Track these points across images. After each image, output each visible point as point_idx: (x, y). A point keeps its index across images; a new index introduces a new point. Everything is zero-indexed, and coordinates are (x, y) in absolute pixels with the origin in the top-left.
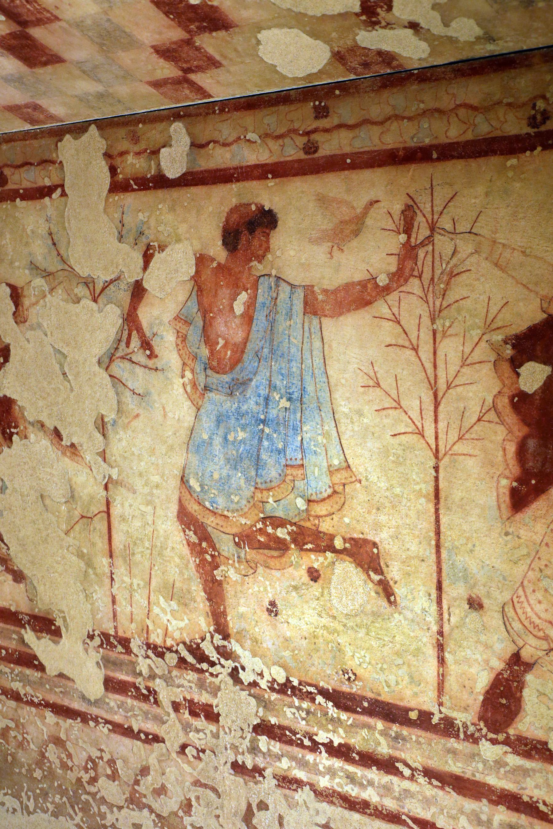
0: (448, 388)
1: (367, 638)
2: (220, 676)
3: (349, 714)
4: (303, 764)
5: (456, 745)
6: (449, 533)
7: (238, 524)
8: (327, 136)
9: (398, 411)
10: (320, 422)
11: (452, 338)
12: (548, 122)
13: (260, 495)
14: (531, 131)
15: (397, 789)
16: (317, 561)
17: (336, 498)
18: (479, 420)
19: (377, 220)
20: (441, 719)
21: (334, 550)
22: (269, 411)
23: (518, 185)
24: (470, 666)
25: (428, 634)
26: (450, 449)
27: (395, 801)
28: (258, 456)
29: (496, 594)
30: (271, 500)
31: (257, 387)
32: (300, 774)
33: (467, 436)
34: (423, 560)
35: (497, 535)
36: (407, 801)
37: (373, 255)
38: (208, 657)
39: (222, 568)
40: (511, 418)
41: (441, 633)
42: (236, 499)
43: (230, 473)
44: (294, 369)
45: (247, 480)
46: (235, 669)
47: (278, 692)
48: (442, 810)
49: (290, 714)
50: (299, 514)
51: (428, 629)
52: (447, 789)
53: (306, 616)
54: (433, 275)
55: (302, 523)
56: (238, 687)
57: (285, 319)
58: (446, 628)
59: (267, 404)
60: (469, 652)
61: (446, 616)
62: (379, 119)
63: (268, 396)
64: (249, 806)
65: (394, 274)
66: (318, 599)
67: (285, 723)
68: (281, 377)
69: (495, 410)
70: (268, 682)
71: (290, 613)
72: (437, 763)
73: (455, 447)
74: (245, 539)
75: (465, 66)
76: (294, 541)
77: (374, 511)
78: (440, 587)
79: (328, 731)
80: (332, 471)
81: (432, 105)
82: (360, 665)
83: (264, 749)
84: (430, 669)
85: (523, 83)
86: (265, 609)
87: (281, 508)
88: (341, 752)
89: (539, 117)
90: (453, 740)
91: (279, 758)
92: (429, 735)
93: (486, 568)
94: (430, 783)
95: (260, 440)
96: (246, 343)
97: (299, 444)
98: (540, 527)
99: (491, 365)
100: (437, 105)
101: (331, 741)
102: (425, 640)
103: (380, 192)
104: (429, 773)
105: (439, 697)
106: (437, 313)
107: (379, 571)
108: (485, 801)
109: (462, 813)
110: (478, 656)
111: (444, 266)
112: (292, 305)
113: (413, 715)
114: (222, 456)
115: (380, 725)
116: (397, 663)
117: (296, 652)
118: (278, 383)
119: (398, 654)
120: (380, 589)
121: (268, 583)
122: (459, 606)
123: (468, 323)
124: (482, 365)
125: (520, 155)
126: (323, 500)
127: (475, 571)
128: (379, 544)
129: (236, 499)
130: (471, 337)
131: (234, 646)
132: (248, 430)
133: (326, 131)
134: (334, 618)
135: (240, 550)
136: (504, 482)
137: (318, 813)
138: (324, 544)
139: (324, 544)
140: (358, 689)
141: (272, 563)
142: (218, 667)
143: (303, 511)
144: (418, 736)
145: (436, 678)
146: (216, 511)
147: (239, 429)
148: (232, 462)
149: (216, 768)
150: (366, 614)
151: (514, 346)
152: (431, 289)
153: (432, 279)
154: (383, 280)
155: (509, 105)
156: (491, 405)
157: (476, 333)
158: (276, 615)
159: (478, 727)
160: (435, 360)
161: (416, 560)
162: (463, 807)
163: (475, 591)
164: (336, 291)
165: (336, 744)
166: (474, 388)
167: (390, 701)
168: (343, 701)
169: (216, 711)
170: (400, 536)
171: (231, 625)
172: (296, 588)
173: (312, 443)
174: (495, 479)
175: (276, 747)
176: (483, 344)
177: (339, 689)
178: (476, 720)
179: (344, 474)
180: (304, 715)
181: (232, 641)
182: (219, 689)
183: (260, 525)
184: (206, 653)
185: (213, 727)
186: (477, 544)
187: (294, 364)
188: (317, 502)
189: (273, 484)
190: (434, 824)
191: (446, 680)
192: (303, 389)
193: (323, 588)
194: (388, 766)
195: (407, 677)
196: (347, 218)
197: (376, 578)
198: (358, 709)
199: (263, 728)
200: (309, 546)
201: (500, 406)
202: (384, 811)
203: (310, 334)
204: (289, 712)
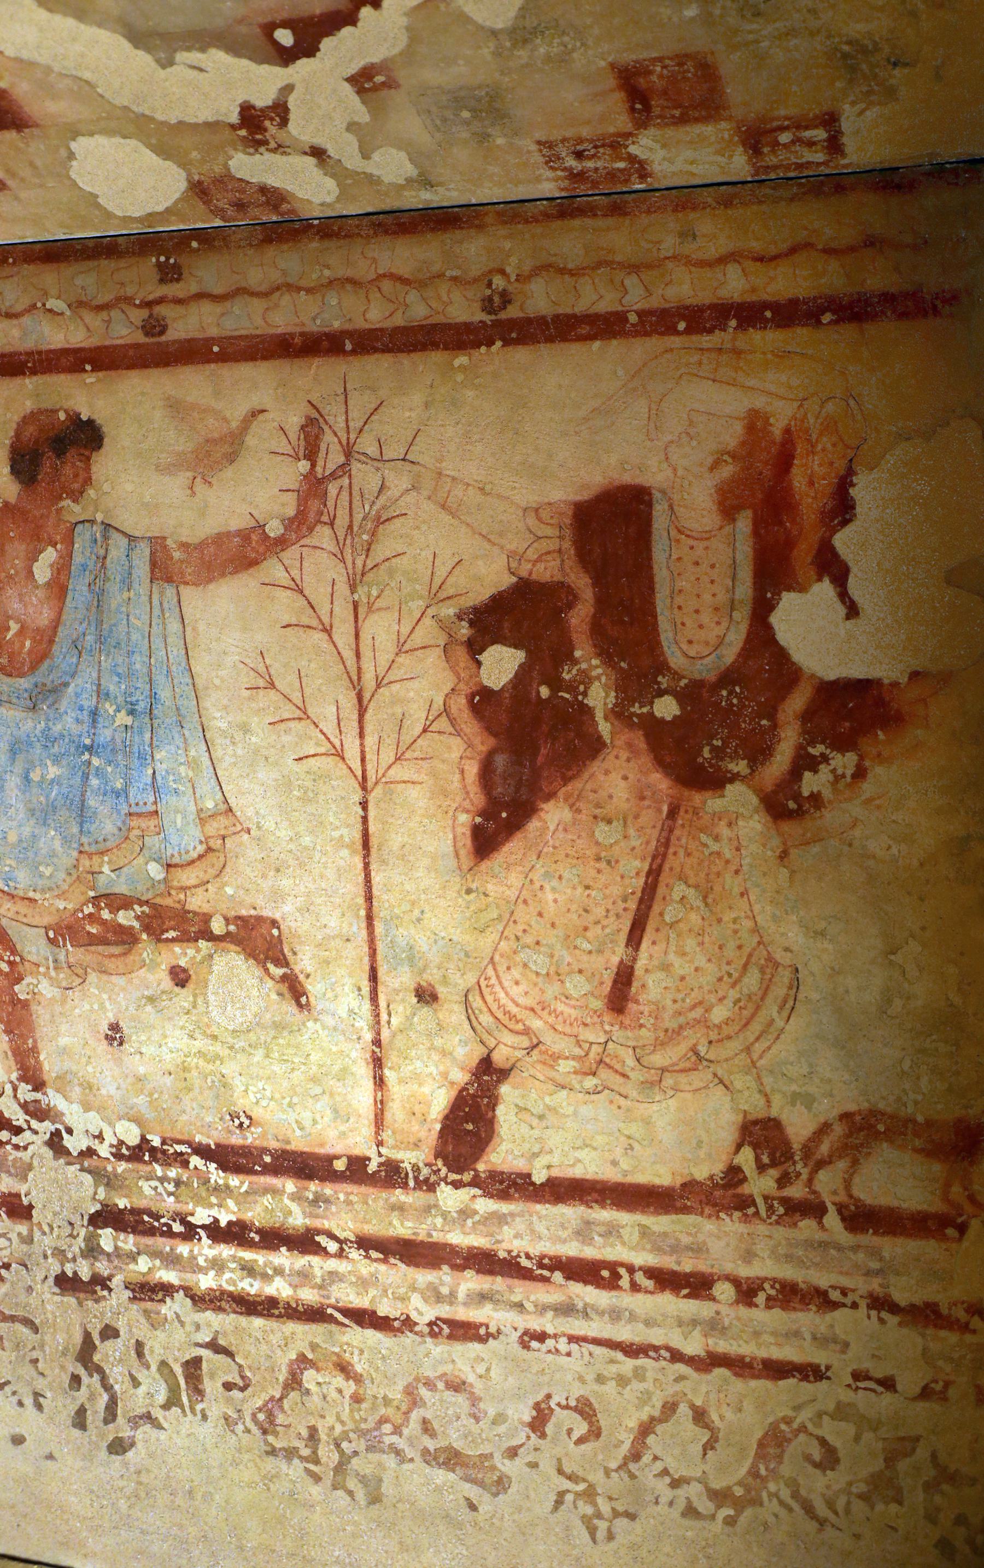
0: (379, 686)
1: (267, 1062)
2: (31, 1148)
3: (242, 1177)
4: (172, 1260)
5: (403, 1198)
6: (385, 897)
7: (53, 909)
8: (180, 310)
9: (303, 723)
10: (182, 745)
11: (382, 614)
12: (509, 307)
13: (87, 863)
14: (488, 318)
15: (318, 1273)
16: (184, 955)
17: (211, 857)
18: (425, 731)
19: (260, 438)
20: (380, 1165)
21: (212, 938)
22: (97, 731)
23: (470, 393)
24: (420, 1085)
25: (358, 1046)
26: (384, 775)
27: (316, 1291)
28: (83, 801)
29: (455, 977)
30: (106, 869)
31: (77, 695)
32: (169, 1276)
33: (407, 755)
34: (348, 940)
35: (455, 895)
36: (334, 1287)
37: (260, 490)
38: (9, 1121)
39: (28, 980)
40: (471, 726)
41: (377, 1042)
42: (48, 872)
43: (37, 831)
44: (138, 666)
45: (66, 841)
46: (57, 1134)
47: (129, 1159)
48: (386, 1291)
49: (150, 1190)
50: (153, 886)
51: (359, 1038)
52: (392, 1260)
53: (169, 1040)
54: (351, 521)
55: (158, 900)
56: (62, 1161)
57: (121, 590)
58: (385, 1034)
59: (94, 721)
60: (418, 1064)
61: (384, 1017)
62: (263, 288)
63: (96, 708)
64: (87, 1336)
65: (292, 520)
66: (187, 1013)
67: (142, 1204)
68: (117, 679)
69: (448, 716)
70: (111, 1146)
71: (143, 1038)
72: (376, 1228)
73: (392, 772)
74: (66, 932)
75: (389, 219)
76: (147, 928)
77: (272, 873)
78: (373, 977)
79: (211, 1206)
80: (203, 818)
81: (342, 272)
82: (257, 1103)
83: (108, 1248)
84: (362, 1096)
85: (473, 250)
86: (102, 1037)
87: (123, 879)
88: (235, 1234)
89: (496, 299)
90: (398, 1191)
91: (133, 1257)
92: (363, 1189)
93: (441, 943)
94: (367, 1257)
95: (86, 777)
96: (56, 627)
97: (149, 781)
98: (515, 879)
99: (439, 651)
100: (349, 273)
101: (216, 1221)
102: (354, 1055)
103: (268, 397)
104: (365, 1243)
105: (377, 1133)
106: (358, 577)
107: (281, 961)
108: (445, 1268)
109: (414, 1289)
110: (433, 1069)
111: (367, 507)
112: (131, 567)
113: (340, 1165)
114: (21, 806)
115: (290, 1185)
116: (313, 1093)
117: (156, 1096)
118: (112, 688)
119: (314, 1080)
120: (284, 988)
121: (105, 996)
122: (403, 1000)
123: (405, 591)
124: (427, 651)
125: (472, 351)
126: (193, 862)
127: (425, 948)
128: (281, 922)
129: (48, 872)
130: (410, 611)
131: (53, 1098)
132: (64, 762)
133: (179, 301)
134: (215, 1037)
135: (57, 950)
136: (463, 818)
137: (198, 1327)
138: (195, 929)
139: (195, 929)
140: (255, 1139)
141: (111, 965)
142: (27, 1134)
143: (159, 882)
144: (347, 1194)
145: (373, 1108)
146: (15, 893)
147: (49, 763)
148: (38, 813)
149: (30, 1289)
150: (264, 1028)
151: (472, 624)
152: (348, 542)
153: (350, 527)
154: (274, 529)
155: (455, 279)
156: (442, 708)
157: (417, 606)
158: (121, 1044)
159: (435, 1168)
160: (357, 645)
161: (338, 941)
162: (415, 1280)
163: (425, 976)
164: (201, 546)
165: (223, 1224)
166: (415, 684)
167: (306, 1149)
168: (230, 1158)
169: (25, 1201)
170: (312, 908)
171: (46, 1067)
172: (151, 1000)
173: (171, 778)
174: (451, 813)
175: (129, 1242)
176: (427, 621)
177: (224, 1141)
178: (431, 1159)
179: (223, 821)
180: (171, 1188)
181: (50, 1091)
182: (30, 1167)
183: (89, 909)
184: (7, 1115)
185: (23, 1228)
186: (427, 909)
187: (137, 658)
188: (182, 866)
189: (109, 845)
190: (374, 1312)
191: (386, 1108)
192: (153, 696)
193: (195, 996)
194: (305, 1242)
195: (328, 1112)
196: (216, 435)
197: (278, 972)
198: (257, 1168)
199: (106, 1217)
200: (172, 934)
201: (454, 710)
202: (300, 1308)
203: (163, 611)
204: (146, 1187)
